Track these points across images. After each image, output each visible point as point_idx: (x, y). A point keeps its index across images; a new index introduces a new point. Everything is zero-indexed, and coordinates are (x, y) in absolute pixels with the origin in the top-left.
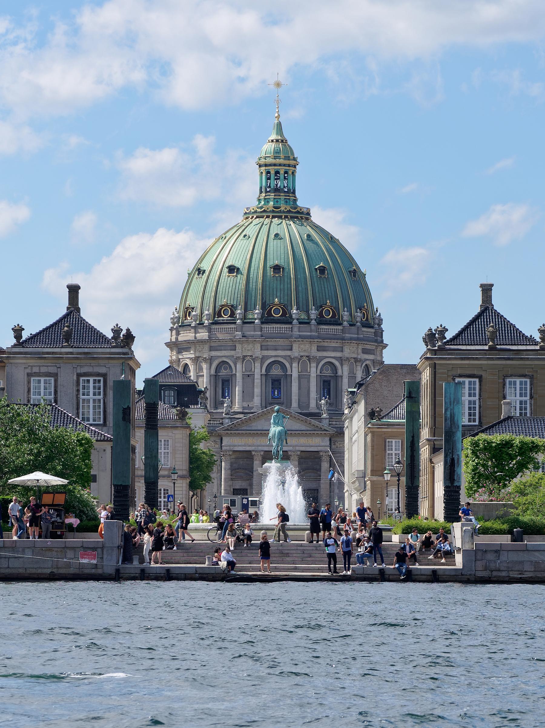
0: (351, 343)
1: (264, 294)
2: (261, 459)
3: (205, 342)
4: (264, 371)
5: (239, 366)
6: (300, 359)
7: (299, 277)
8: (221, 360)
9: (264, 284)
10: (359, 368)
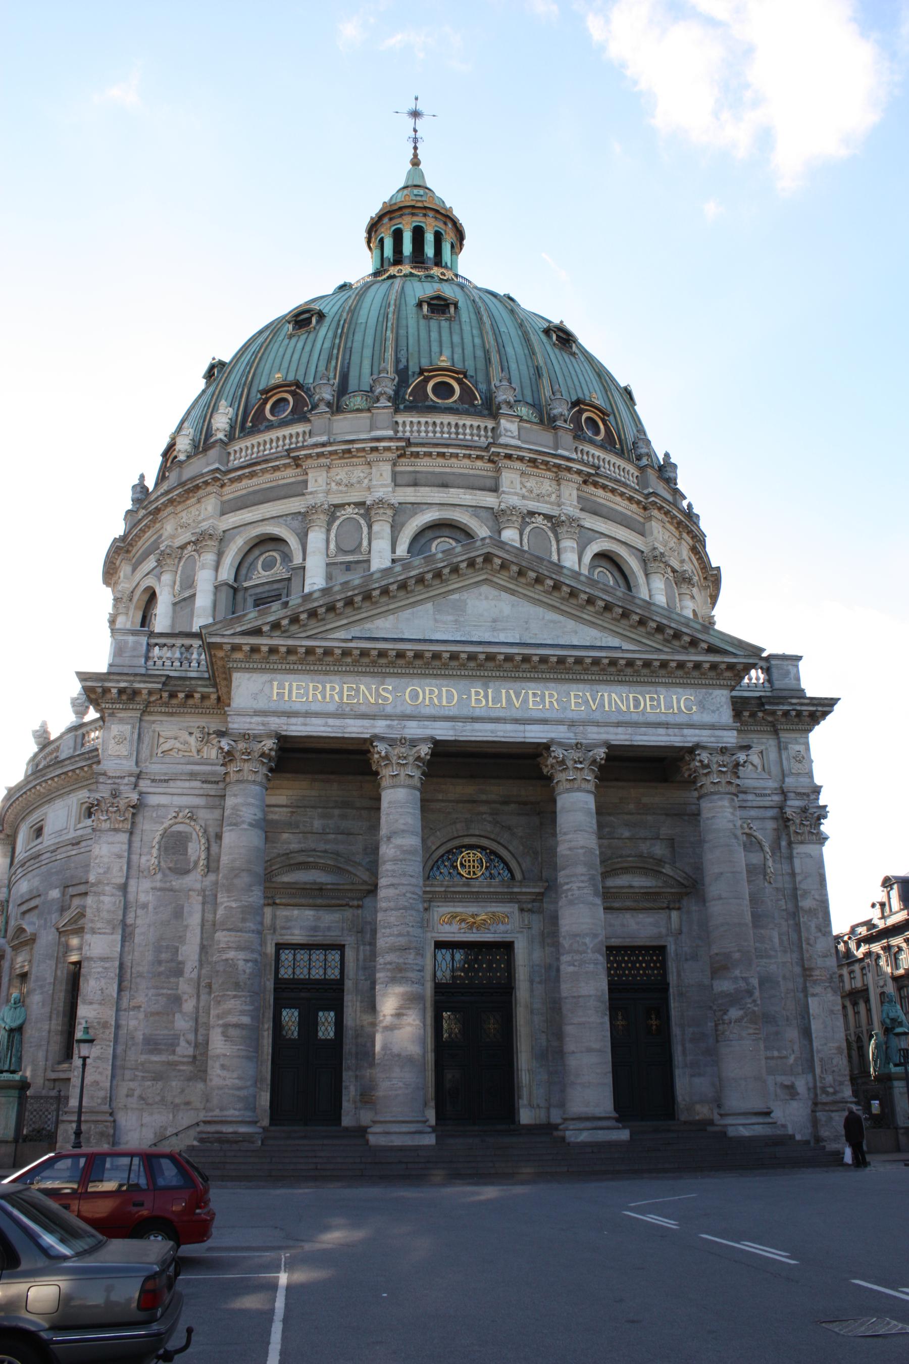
0: (667, 513)
2: (416, 782)
3: (206, 483)
4: (402, 550)
5: (316, 538)
6: (524, 524)
7: (502, 330)
9: (402, 332)
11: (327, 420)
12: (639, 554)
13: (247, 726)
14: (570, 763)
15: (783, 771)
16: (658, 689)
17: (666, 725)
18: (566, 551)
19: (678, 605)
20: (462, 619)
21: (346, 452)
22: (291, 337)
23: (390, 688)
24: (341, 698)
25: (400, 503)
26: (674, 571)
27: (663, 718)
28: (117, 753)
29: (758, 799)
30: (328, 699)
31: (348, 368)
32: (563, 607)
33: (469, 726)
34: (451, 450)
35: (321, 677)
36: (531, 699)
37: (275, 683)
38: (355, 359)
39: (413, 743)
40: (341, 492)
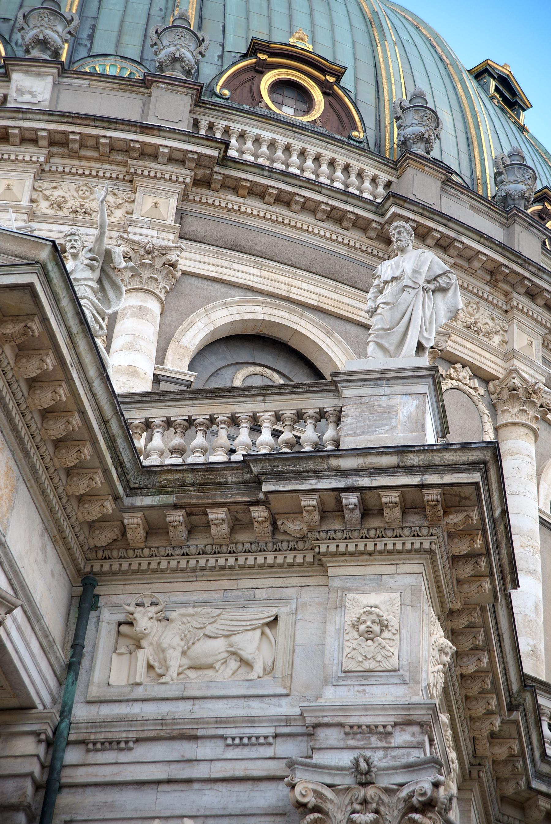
29: (231, 753)
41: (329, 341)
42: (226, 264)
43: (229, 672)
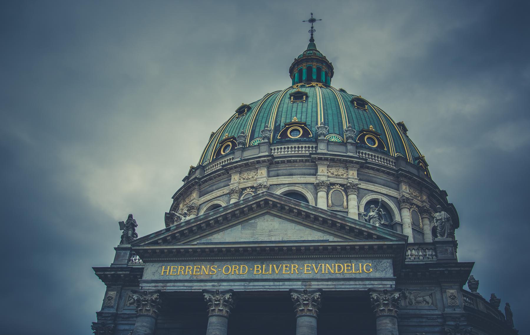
0: (410, 178)
1: (279, 118)
2: (224, 313)
3: (193, 185)
8: (210, 204)
9: (280, 109)
10: (427, 221)
11: (241, 151)
12: (395, 200)
13: (148, 288)
14: (301, 301)
15: (444, 304)
16: (352, 261)
17: (355, 279)
18: (351, 200)
19: (421, 224)
20: (255, 232)
21: (247, 165)
22: (237, 118)
23: (216, 266)
24: (193, 273)
25: (270, 185)
26: (417, 206)
27: (354, 276)
28: (109, 305)
29: (429, 321)
30: (186, 274)
31: (255, 128)
32: (304, 223)
33: (251, 284)
34: (293, 159)
35: (185, 263)
36: (284, 269)
37: (164, 267)
38: (259, 124)
39: (224, 293)
40: (245, 182)
41: (389, 202)
42: (368, 185)
43: (424, 304)
